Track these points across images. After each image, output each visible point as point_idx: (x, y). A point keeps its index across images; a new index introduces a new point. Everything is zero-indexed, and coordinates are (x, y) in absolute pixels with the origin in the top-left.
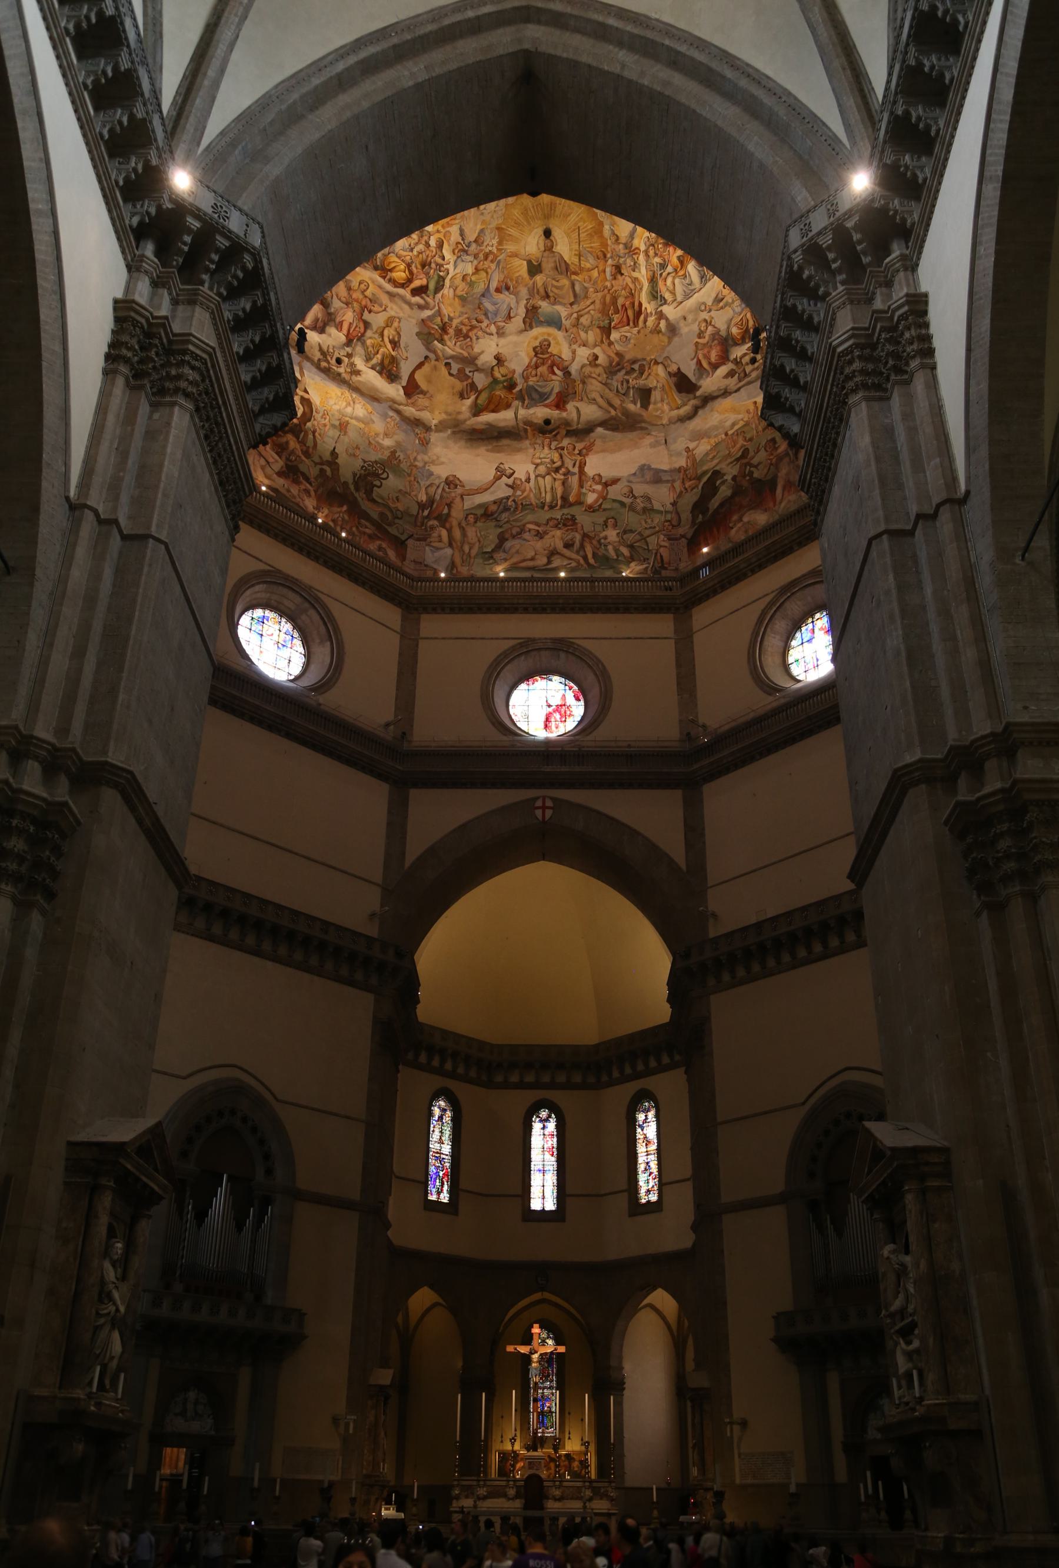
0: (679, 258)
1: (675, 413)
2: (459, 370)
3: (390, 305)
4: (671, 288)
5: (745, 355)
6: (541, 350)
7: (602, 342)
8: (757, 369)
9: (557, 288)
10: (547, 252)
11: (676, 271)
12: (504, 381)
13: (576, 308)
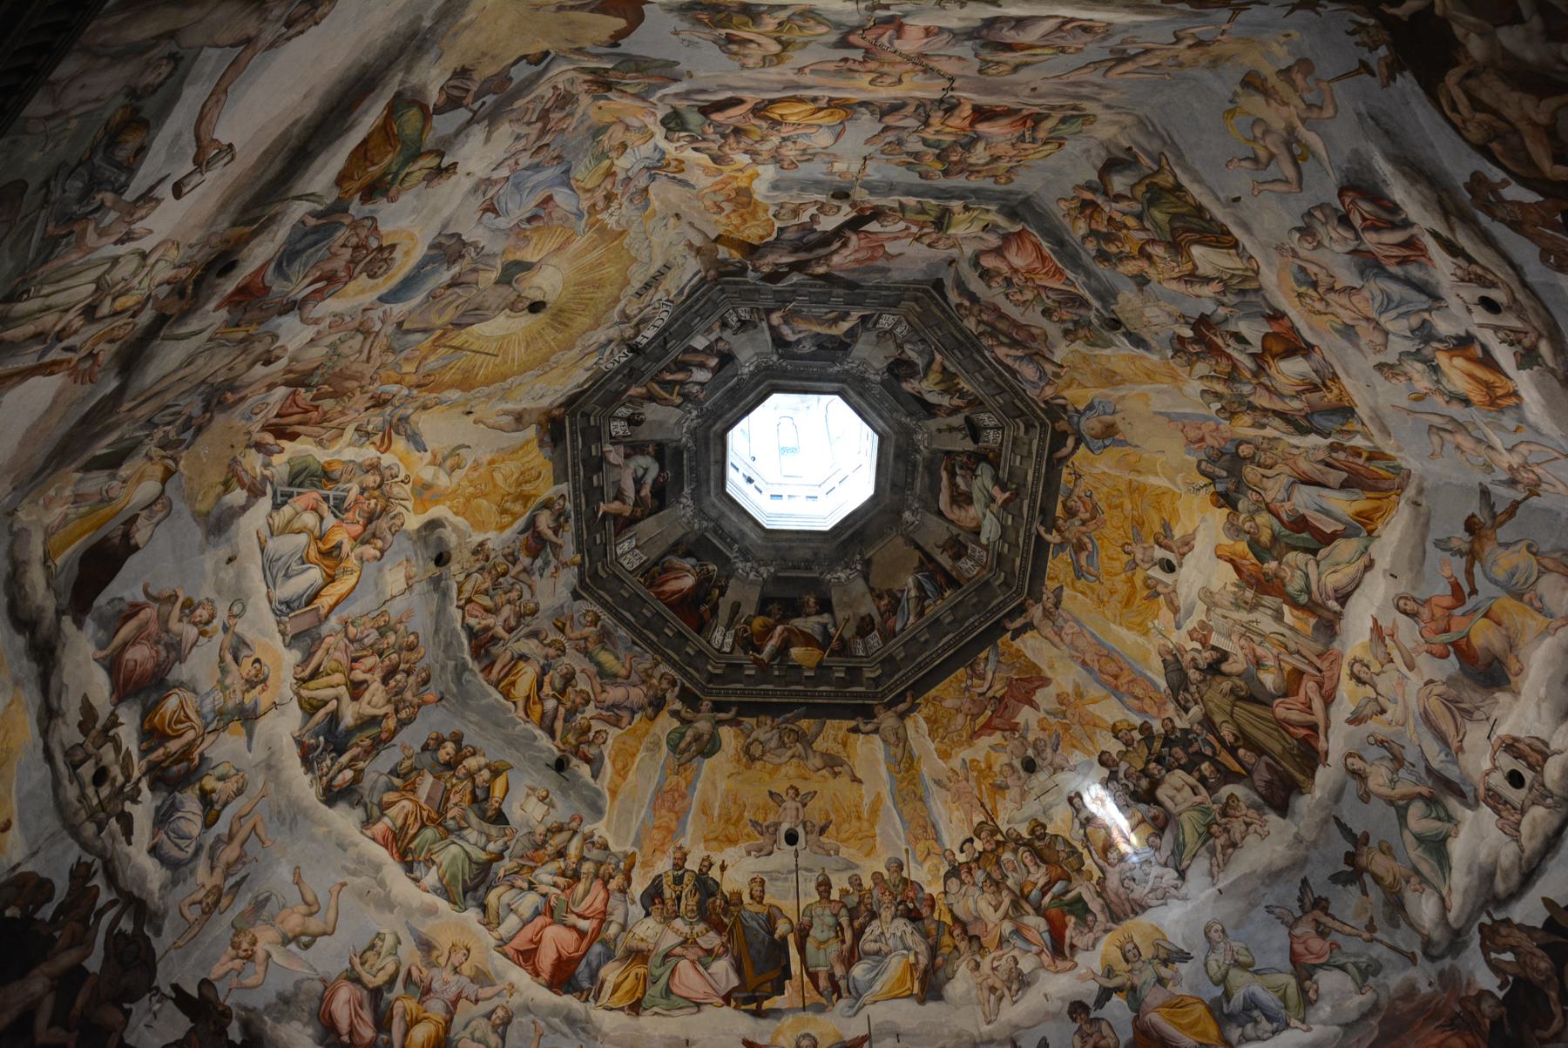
0: (339, 546)
1: (40, 552)
2: (511, 79)
3: (791, 76)
4: (296, 525)
5: (118, 748)
6: (375, 258)
7: (290, 371)
8: (83, 797)
9: (451, 303)
10: (513, 297)
11: (321, 538)
12: (396, 175)
13: (390, 329)
